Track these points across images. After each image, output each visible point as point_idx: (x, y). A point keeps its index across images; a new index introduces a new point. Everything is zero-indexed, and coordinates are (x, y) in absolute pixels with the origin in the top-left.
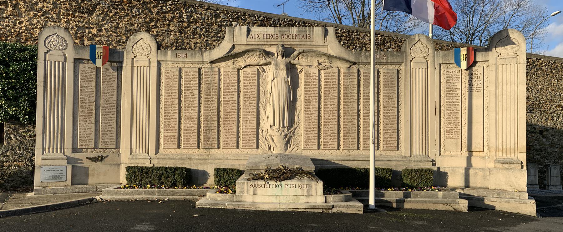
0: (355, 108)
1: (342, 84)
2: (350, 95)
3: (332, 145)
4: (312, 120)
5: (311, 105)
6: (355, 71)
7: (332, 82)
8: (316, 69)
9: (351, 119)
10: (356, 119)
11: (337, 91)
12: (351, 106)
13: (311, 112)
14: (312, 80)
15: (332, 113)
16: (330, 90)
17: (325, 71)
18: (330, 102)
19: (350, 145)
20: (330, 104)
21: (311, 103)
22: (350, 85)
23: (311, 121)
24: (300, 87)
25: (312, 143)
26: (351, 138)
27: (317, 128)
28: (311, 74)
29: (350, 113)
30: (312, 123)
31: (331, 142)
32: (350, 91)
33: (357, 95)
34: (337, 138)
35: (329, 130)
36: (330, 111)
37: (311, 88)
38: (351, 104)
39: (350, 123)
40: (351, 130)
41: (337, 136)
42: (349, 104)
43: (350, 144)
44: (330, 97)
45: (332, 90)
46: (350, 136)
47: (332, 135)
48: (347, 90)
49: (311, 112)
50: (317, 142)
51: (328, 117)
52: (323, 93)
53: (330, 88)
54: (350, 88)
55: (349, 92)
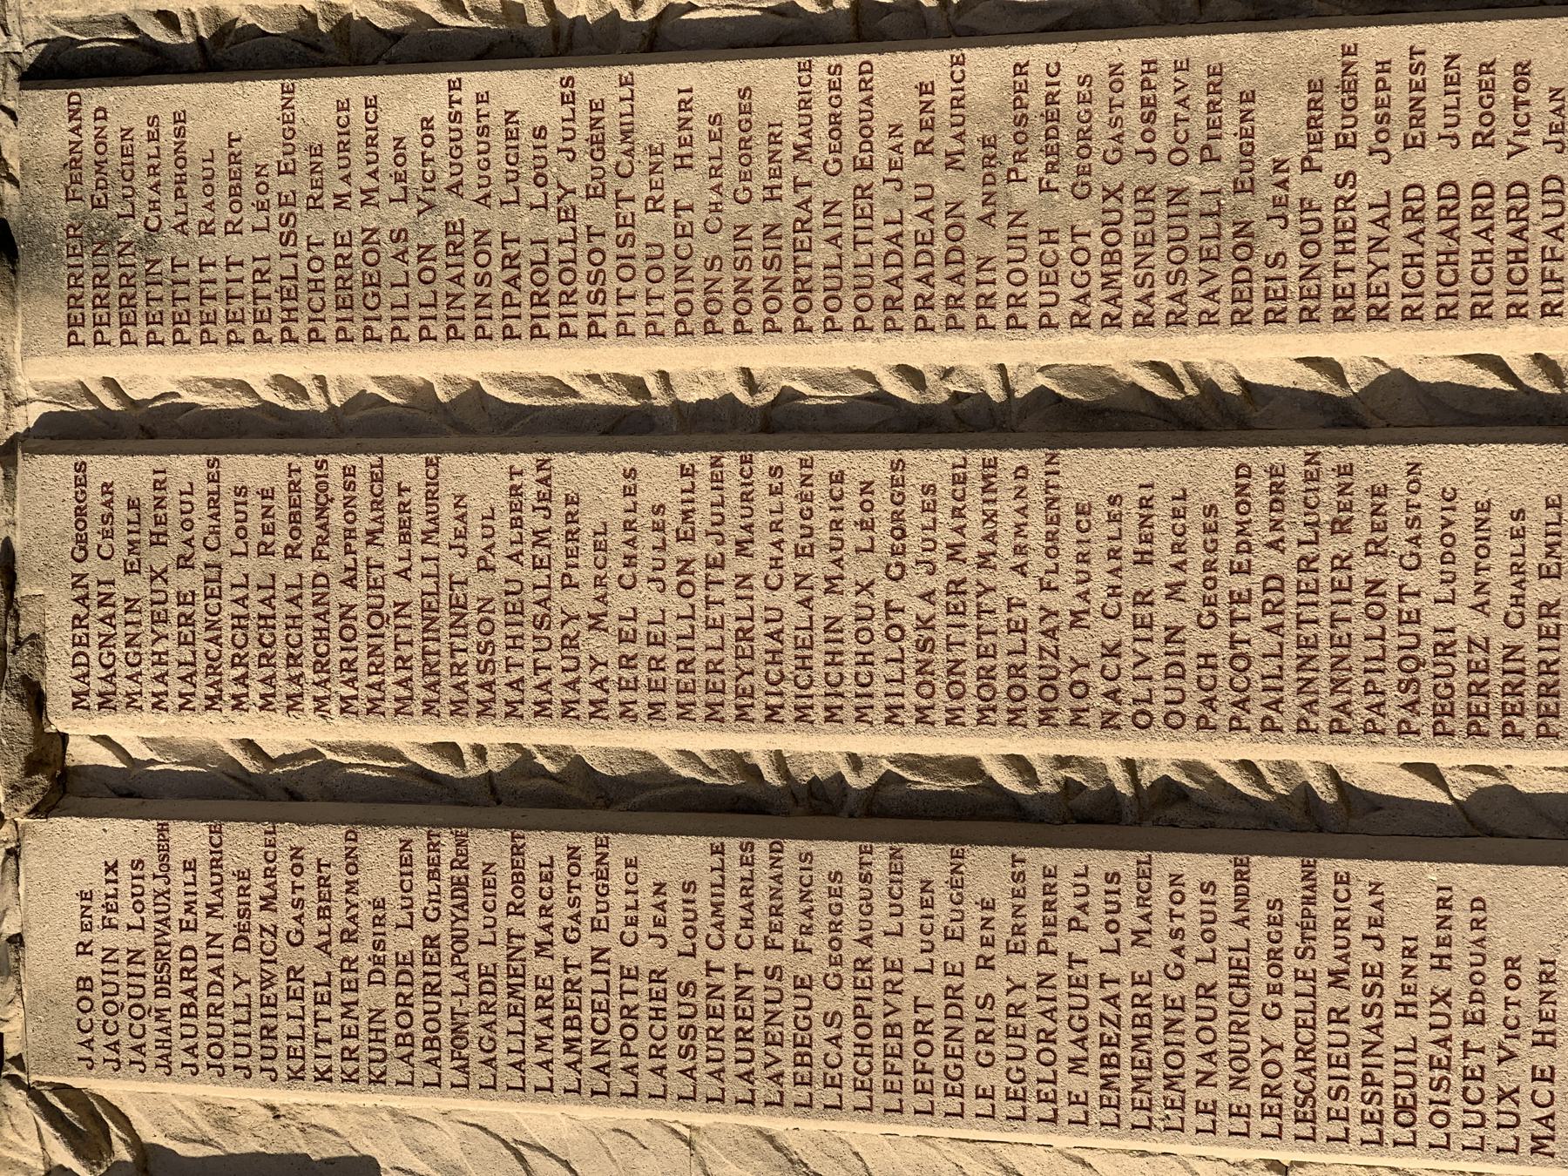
0: (728, 103)
1: (298, 364)
2: (476, 218)
3: (1502, 550)
4: (969, 950)
5: (690, 970)
6: (57, 138)
7: (255, 567)
8: (29, 860)
9: (946, 186)
10: (931, 64)
11: (407, 468)
12: (685, 186)
13: (815, 964)
14: (226, 926)
15: (819, 566)
16: (396, 591)
17: (58, 681)
18: (621, 602)
19: (1495, 166)
20: (647, 599)
21: (645, 956)
22: (310, 226)
23: (976, 984)
24: (366, 1148)
25: (1456, 981)
26: (1332, 160)
27: (1125, 862)
28: (121, 940)
29: (827, 190)
30: (1027, 967)
31: (1427, 580)
32: (404, 214)
33: (474, 81)
34: (1332, 456)
35: (1165, 612)
36: (786, 598)
37: (362, 951)
38: (639, 186)
39: (1023, 195)
40: (1164, 175)
41: (1292, 458)
42: (653, 229)
43: (1469, 166)
44: (514, 590)
45: (390, 553)
46: (1301, 185)
47: (1265, 562)
48: (391, 270)
49: (815, 964)
50: (1433, 872)
51: (894, 632)
52: (464, 735)
53: (358, 597)
54: (357, 218)
55: (433, 231)
